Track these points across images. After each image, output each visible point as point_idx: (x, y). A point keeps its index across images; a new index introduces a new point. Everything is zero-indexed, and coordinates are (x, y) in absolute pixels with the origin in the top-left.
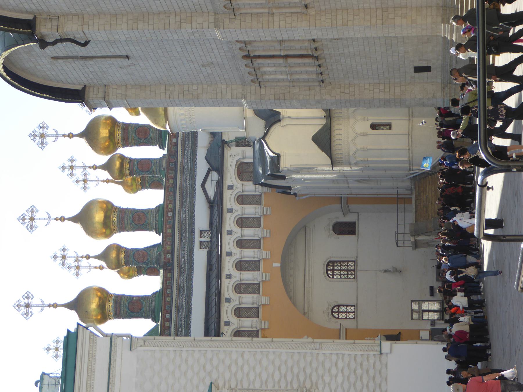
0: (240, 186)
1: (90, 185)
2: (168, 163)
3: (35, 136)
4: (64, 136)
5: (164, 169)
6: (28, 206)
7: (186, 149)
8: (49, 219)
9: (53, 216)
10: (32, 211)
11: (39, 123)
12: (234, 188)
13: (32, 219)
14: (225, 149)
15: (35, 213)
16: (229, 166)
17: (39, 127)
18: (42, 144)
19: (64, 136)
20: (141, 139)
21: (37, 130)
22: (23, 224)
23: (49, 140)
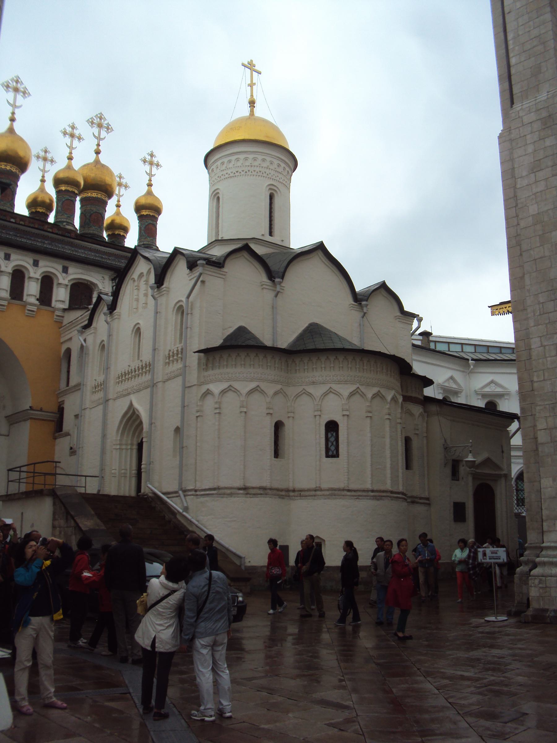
0: (66, 282)
1: (41, 163)
2: (70, 231)
3: (101, 118)
4: (98, 145)
5: (64, 226)
6: (30, 90)
7: (86, 252)
8: (14, 106)
9: (17, 111)
10: (25, 93)
11: (112, 125)
12: (64, 275)
13: (16, 90)
14: (112, 273)
15: (22, 94)
16: (92, 274)
17: (108, 125)
18: (92, 123)
19: (98, 145)
20: (90, 216)
21: (106, 122)
22: (12, 80)
23: (96, 130)
